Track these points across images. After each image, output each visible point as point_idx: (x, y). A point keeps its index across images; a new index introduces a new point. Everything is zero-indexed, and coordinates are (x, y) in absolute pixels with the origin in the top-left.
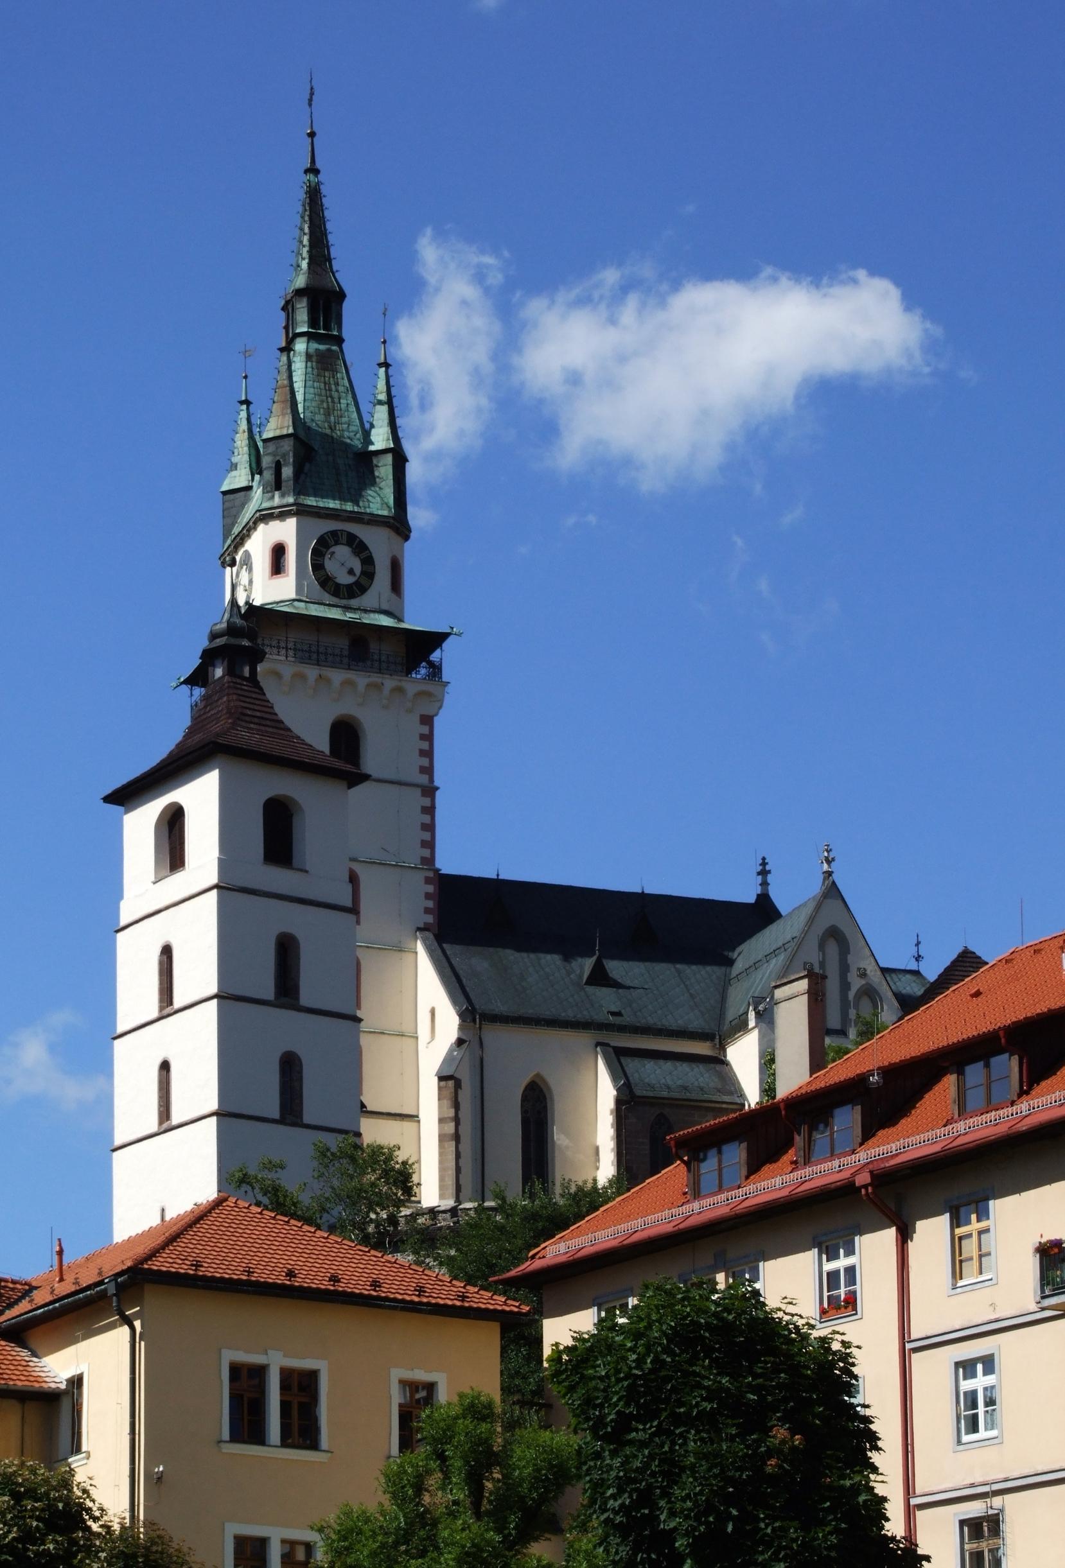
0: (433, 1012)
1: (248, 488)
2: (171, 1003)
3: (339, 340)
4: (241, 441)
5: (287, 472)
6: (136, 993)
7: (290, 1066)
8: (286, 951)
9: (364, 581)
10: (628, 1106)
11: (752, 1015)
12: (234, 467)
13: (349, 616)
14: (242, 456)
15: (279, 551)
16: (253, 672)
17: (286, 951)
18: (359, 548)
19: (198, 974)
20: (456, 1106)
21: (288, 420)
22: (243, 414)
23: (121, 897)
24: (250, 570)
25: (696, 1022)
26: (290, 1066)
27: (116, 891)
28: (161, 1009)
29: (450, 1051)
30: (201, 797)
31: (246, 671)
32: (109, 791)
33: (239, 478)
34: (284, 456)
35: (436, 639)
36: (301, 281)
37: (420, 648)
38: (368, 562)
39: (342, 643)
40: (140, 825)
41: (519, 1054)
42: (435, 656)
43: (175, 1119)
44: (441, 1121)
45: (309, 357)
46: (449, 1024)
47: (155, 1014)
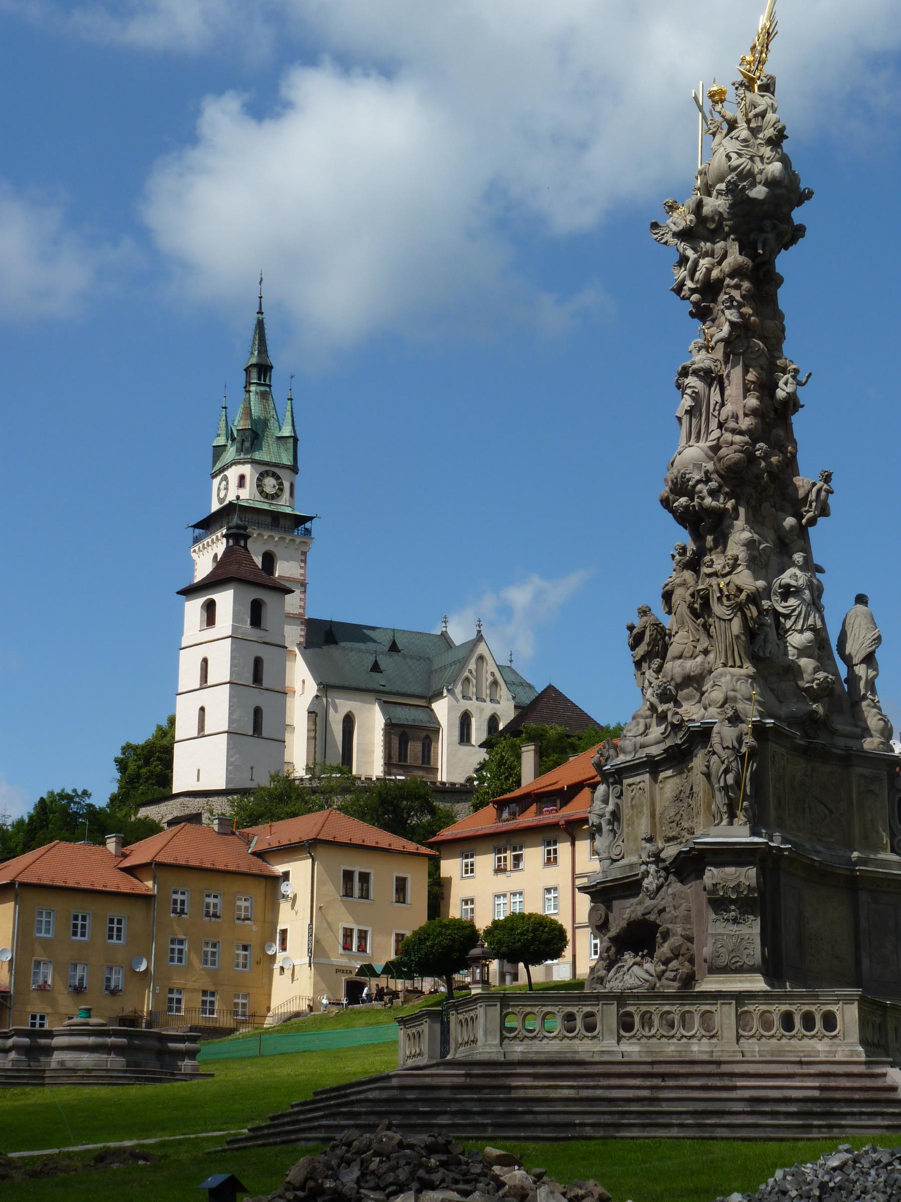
0: (304, 681)
1: (226, 446)
2: (206, 682)
3: (270, 386)
4: (222, 425)
5: (247, 444)
6: (188, 676)
7: (258, 712)
8: (258, 663)
9: (279, 493)
10: (390, 728)
11: (445, 691)
12: (219, 435)
13: (272, 508)
14: (223, 431)
15: (242, 478)
16: (246, 543)
17: (258, 663)
18: (278, 478)
19: (220, 671)
20: (315, 724)
21: (249, 422)
22: (224, 413)
23: (182, 635)
24: (227, 483)
25: (418, 691)
26: (258, 712)
27: (181, 633)
28: (201, 685)
29: (313, 700)
30: (225, 599)
31: (242, 543)
32: (179, 590)
33: (221, 441)
34: (247, 438)
35: (310, 519)
36: (254, 360)
37: (300, 520)
38: (281, 484)
39: (269, 520)
40: (194, 608)
41: (344, 705)
42: (308, 525)
43: (206, 732)
44: (308, 730)
45: (257, 393)
46: (312, 688)
47: (198, 687)
